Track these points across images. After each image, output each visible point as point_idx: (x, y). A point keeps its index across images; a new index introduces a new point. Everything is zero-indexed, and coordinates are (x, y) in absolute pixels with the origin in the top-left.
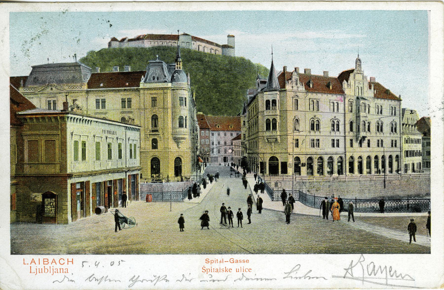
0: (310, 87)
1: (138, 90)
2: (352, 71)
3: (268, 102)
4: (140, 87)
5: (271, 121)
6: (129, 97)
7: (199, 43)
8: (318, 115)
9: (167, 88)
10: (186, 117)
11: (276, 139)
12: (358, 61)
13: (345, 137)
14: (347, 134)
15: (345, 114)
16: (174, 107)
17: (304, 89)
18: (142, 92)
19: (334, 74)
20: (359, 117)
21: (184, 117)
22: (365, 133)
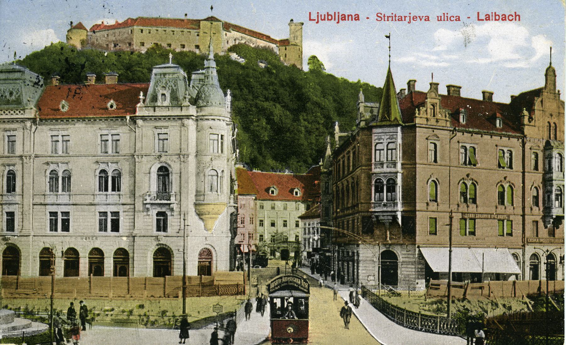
1: (134, 120)
2: (537, 93)
4: (137, 114)
5: (385, 183)
9: (188, 117)
10: (223, 171)
11: (395, 218)
12: (550, 73)
13: (523, 216)
14: (527, 210)
15: (523, 173)
18: (140, 122)
19: (503, 97)
20: (551, 180)
21: (219, 172)
22: (561, 210)
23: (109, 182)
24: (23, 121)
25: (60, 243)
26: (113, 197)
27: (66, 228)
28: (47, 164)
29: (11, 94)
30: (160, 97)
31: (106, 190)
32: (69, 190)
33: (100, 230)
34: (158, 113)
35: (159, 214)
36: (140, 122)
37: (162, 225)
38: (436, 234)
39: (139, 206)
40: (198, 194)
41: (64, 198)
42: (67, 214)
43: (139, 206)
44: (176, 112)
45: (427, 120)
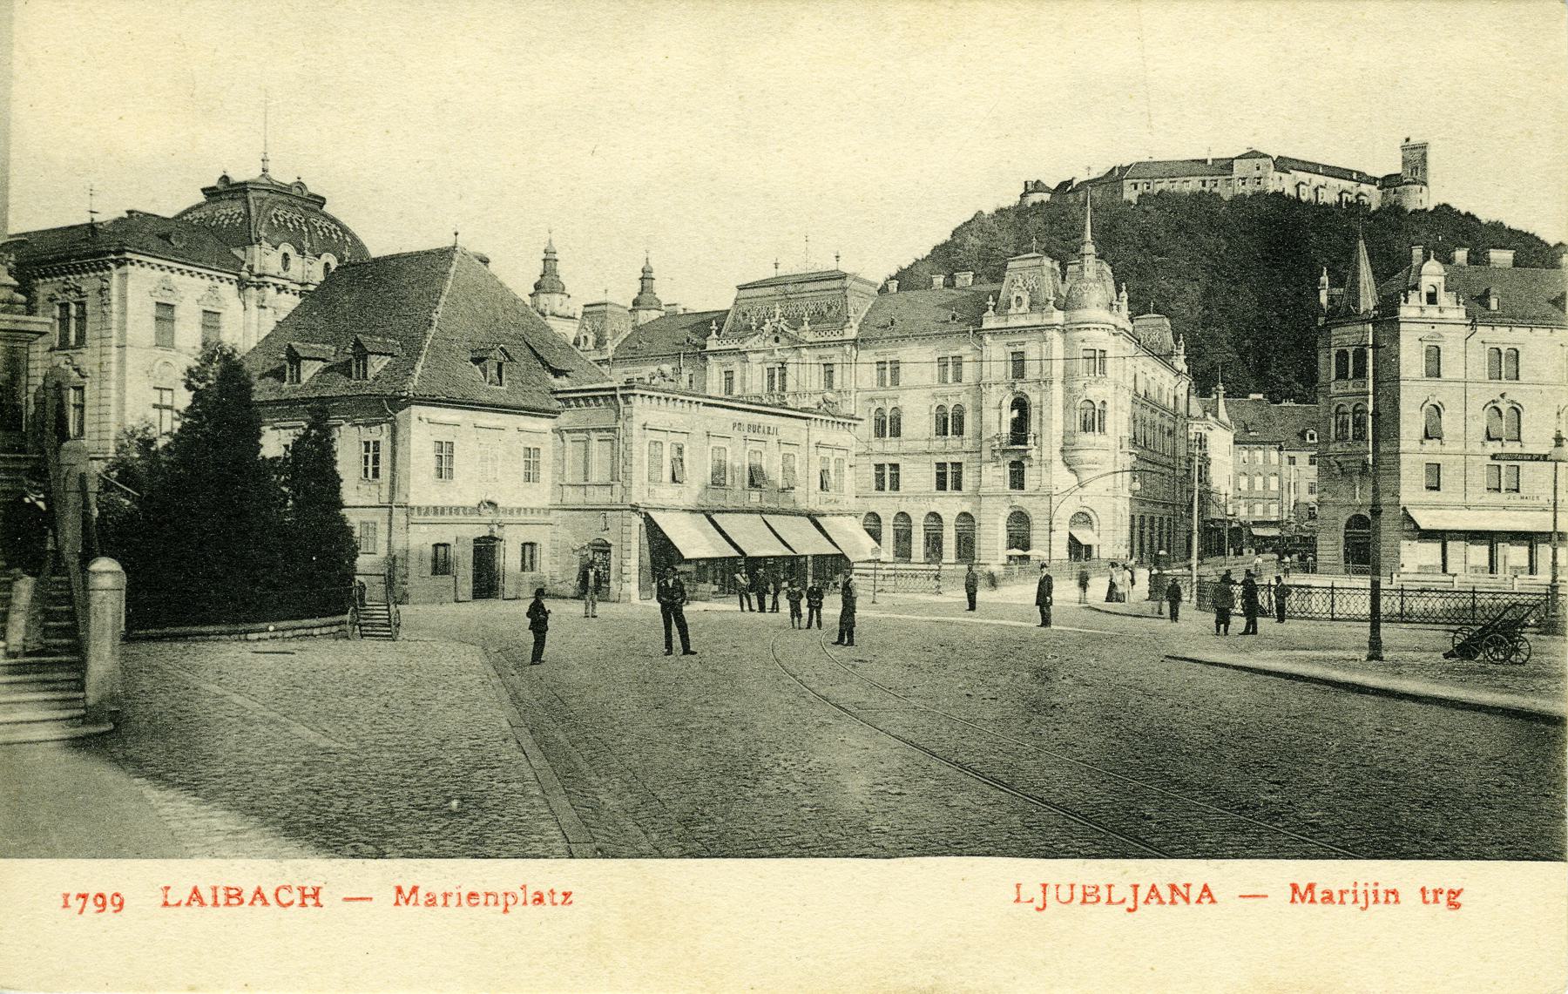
0: (1488, 307)
1: (979, 334)
3: (1342, 355)
6: (956, 353)
7: (1303, 176)
8: (1515, 392)
9: (1052, 326)
16: (1068, 377)
17: (1462, 314)
18: (988, 338)
23: (949, 423)
24: (842, 343)
25: (887, 507)
26: (952, 441)
27: (896, 486)
28: (872, 400)
29: (830, 308)
30: (1013, 303)
31: (946, 434)
32: (898, 435)
33: (938, 489)
34: (1012, 323)
35: (1013, 464)
36: (988, 338)
37: (1017, 481)
38: (1437, 489)
39: (986, 455)
40: (1067, 434)
41: (891, 444)
42: (895, 466)
43: (986, 455)
44: (1036, 319)
45: (1422, 310)
